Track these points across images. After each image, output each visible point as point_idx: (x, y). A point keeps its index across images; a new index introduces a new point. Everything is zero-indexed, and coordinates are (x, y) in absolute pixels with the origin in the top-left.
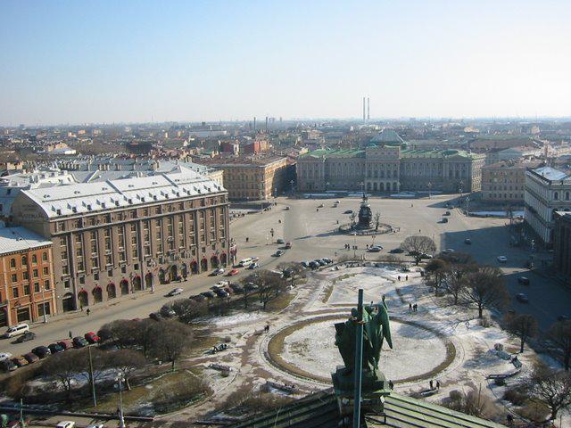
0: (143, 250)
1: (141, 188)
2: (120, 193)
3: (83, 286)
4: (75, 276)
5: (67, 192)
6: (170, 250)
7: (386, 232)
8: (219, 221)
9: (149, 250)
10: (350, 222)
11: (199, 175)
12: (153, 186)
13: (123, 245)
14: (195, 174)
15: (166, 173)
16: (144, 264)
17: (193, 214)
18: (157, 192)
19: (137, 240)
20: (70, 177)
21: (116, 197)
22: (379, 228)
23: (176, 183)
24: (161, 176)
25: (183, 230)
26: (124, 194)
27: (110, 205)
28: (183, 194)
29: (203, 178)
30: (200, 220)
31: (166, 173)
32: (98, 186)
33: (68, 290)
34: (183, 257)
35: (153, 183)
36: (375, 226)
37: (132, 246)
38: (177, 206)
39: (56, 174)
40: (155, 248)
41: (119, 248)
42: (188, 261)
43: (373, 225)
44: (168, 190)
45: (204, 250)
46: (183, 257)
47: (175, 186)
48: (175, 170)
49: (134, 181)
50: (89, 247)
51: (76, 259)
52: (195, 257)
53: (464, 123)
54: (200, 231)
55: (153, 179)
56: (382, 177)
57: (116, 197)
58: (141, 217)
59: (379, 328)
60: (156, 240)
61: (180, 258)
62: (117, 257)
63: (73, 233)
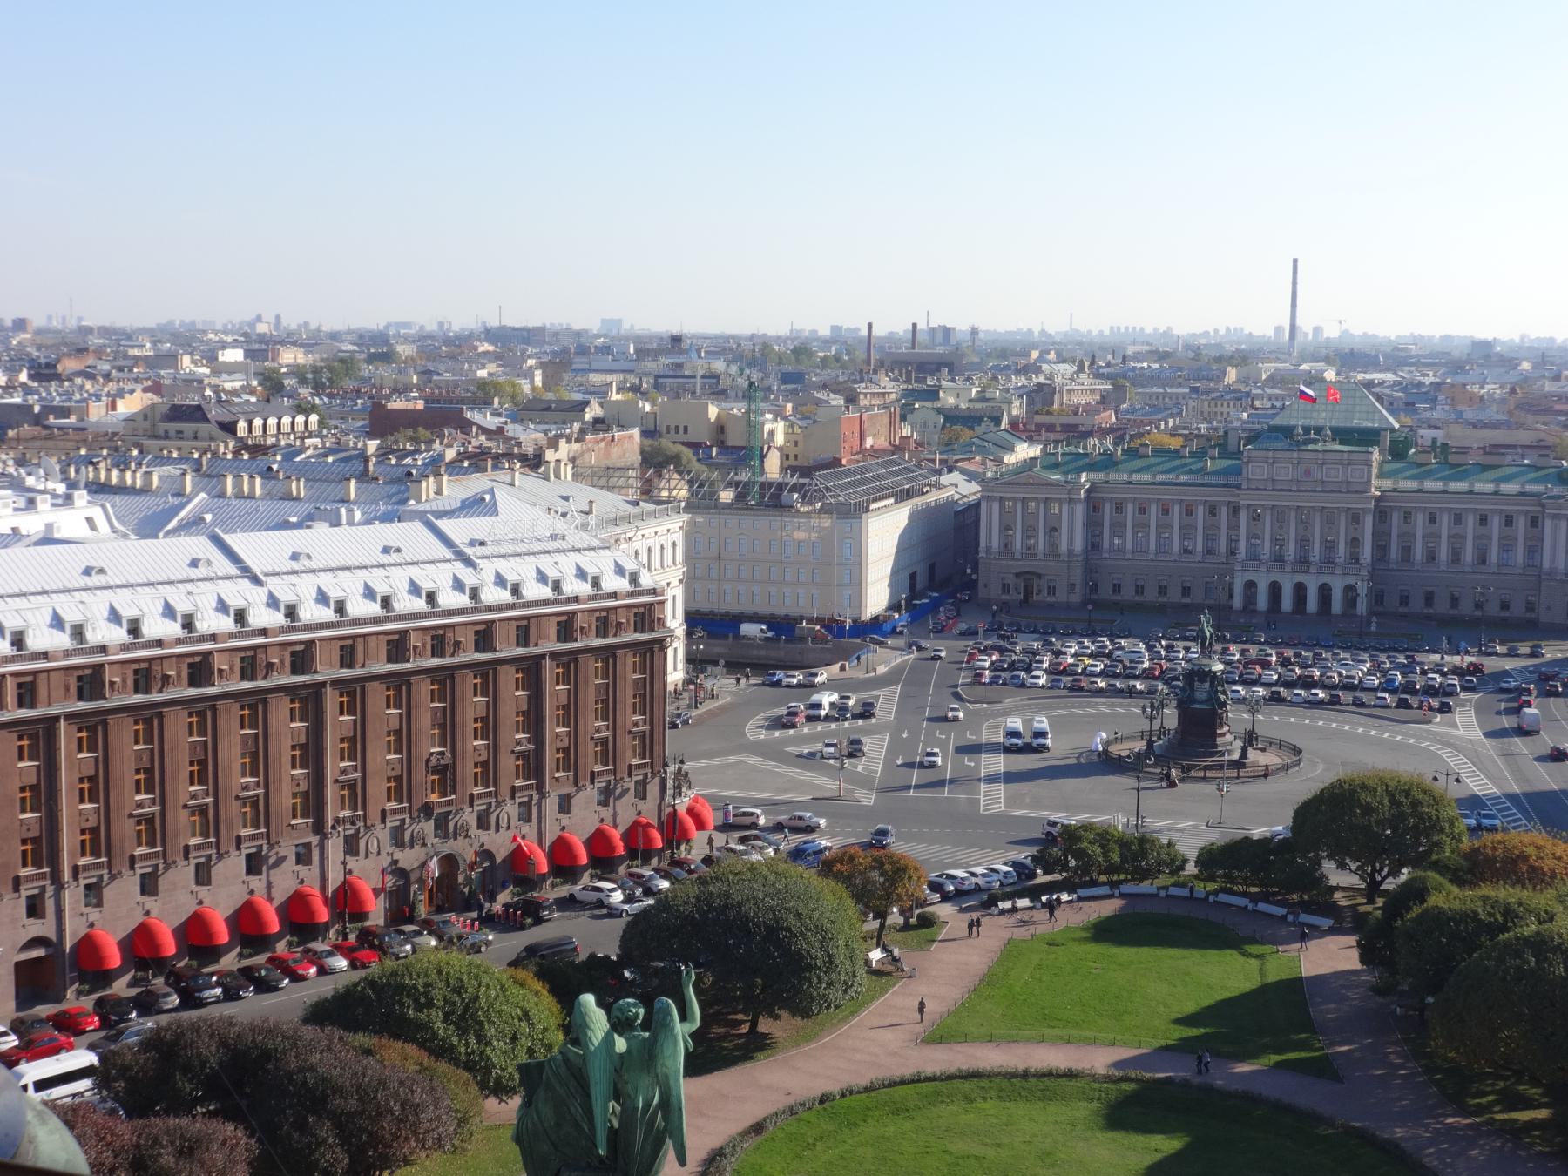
0: (331, 792)
1: (342, 568)
2: (256, 580)
3: (94, 914)
4: (67, 875)
5: (60, 566)
6: (434, 798)
7: (1286, 768)
8: (627, 696)
9: (355, 793)
10: (1145, 725)
11: (561, 526)
12: (386, 559)
13: (254, 773)
14: (547, 524)
15: (441, 514)
16: (335, 846)
17: (531, 670)
18: (394, 582)
19: (311, 753)
20: (97, 513)
21: (239, 593)
22: (1253, 756)
23: (469, 551)
24: (417, 527)
25: (488, 726)
26: (273, 584)
27: (211, 622)
28: (493, 595)
29: (577, 538)
30: (555, 691)
31: (441, 514)
32: (173, 552)
33: (36, 928)
34: (483, 823)
35: (386, 550)
36: (1239, 744)
37: (290, 777)
38: (467, 638)
39: (44, 503)
40: (377, 788)
41: (239, 781)
42: (500, 844)
43: (1230, 743)
44: (439, 578)
45: (565, 805)
46: (483, 823)
47: (469, 562)
48: (477, 505)
49: (322, 541)
50: (125, 770)
51: (73, 812)
52: (529, 830)
53: (1484, 355)
54: (555, 731)
55: (391, 532)
56: (1303, 560)
57: (239, 593)
58: (327, 670)
60: (383, 758)
61: (474, 830)
62: (181, 820)
63: (69, 717)
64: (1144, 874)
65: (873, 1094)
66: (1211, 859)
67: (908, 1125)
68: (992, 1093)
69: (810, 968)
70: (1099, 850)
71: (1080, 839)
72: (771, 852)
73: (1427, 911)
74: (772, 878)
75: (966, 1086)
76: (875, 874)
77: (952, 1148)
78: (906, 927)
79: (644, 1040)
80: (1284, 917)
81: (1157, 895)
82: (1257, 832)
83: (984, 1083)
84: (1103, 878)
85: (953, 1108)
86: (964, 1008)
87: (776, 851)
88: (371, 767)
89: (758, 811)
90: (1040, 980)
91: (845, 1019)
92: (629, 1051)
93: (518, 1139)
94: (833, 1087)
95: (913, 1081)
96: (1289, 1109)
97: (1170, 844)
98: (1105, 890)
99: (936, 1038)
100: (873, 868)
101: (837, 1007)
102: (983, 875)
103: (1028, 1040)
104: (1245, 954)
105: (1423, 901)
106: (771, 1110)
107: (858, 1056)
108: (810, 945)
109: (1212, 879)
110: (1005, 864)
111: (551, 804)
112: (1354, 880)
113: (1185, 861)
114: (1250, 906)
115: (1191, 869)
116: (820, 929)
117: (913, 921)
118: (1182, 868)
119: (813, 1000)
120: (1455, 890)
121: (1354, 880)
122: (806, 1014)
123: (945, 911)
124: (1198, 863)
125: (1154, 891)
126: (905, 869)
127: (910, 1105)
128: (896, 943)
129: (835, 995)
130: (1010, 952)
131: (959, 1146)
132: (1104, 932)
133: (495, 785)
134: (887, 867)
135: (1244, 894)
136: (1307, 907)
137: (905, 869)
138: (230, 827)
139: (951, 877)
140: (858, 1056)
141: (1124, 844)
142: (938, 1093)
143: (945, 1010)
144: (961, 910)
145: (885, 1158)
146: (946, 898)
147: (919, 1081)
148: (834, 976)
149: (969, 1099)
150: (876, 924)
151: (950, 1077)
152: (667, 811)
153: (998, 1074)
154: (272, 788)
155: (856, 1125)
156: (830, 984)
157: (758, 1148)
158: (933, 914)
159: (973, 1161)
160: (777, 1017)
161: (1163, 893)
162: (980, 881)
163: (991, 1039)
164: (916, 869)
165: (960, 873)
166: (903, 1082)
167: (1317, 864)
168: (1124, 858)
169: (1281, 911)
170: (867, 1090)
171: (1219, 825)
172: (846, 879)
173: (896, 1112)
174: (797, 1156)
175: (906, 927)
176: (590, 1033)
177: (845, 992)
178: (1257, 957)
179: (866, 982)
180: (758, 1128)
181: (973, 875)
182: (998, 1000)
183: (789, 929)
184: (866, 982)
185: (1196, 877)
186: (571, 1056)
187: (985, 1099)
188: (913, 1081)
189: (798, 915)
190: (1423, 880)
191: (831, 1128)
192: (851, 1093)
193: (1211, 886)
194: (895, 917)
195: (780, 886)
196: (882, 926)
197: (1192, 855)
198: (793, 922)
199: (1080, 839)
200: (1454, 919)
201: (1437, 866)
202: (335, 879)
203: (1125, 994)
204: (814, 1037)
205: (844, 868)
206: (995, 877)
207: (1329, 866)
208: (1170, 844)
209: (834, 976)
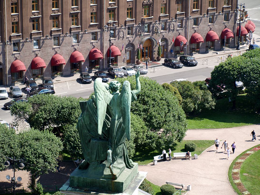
0: (106, 14)
4: (7, 39)
6: (145, 17)
45: (196, 22)
88: (121, 4)
111: (191, 23)
133: (169, 13)
138: (67, 24)
152: (237, 27)
154: (83, 10)
202: (106, 45)
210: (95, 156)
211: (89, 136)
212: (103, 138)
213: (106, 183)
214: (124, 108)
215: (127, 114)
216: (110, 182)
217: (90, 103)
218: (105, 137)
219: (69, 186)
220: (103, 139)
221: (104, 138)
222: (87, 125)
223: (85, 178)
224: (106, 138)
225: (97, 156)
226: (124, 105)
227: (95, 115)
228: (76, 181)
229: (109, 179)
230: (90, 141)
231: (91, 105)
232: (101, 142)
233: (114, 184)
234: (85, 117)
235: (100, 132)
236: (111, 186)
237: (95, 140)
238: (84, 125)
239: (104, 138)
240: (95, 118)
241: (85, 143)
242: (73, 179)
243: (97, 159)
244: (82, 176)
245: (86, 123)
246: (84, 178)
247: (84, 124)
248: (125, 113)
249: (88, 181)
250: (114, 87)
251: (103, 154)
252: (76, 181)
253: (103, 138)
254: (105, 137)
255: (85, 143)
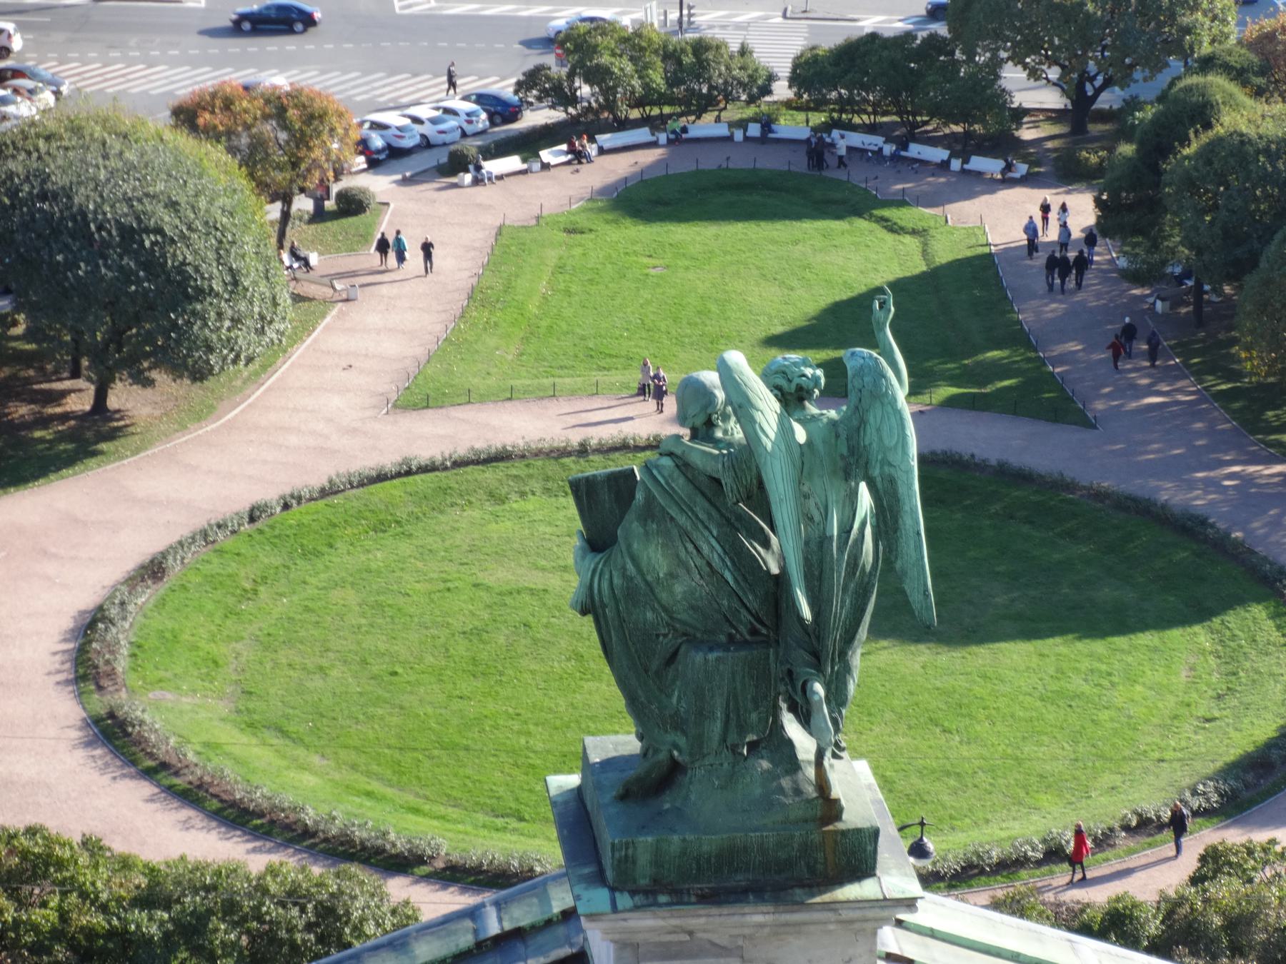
59: (853, 497)
64: (704, 104)
65: (336, 500)
66: (813, 73)
67: (405, 548)
68: (536, 485)
69: (201, 294)
70: (629, 68)
71: (594, 50)
72: (47, 97)
73: (1219, 140)
74: (115, 145)
75: (489, 475)
76: (268, 128)
77: (488, 580)
78: (320, 215)
79: (833, 423)
80: (945, 165)
81: (729, 139)
82: (870, 23)
83: (517, 469)
84: (635, 114)
85: (476, 514)
86: (453, 345)
87: (57, 94)
89: (9, 26)
90: (568, 293)
91: (255, 380)
92: (809, 443)
93: (588, 606)
94: (269, 494)
95: (399, 475)
96: (1022, 477)
97: (744, 51)
98: (643, 134)
99: (418, 396)
100: (266, 117)
101: (250, 360)
102: (434, 121)
103: (573, 393)
104: (894, 228)
105: (1208, 126)
106: (174, 538)
107: (293, 440)
108: (196, 254)
109: (817, 106)
110: (466, 98)
112: (1052, 99)
113: (771, 78)
114: (888, 149)
115: (782, 90)
116: (211, 226)
117: (330, 205)
118: (766, 90)
119: (210, 349)
120: (1260, 107)
121: (1052, 99)
122: (199, 374)
123: (379, 185)
124: (794, 80)
125: (723, 130)
126: (322, 117)
127: (401, 514)
128: (313, 244)
129: (243, 338)
130: (508, 246)
131: (499, 576)
132: (639, 201)
134: (292, 113)
135: (872, 129)
136: (964, 146)
137: (322, 117)
139: (377, 126)
140: (293, 440)
141: (670, 56)
142: (445, 491)
143: (420, 352)
144: (405, 182)
145: (379, 606)
146: (374, 164)
147: (409, 473)
148: (242, 306)
149: (496, 498)
150: (275, 211)
151: (459, 464)
153: (538, 453)
155: (317, 554)
156: (236, 321)
157: (161, 604)
158: (364, 191)
159: (527, 597)
160: (148, 383)
161: (738, 135)
162: (427, 129)
163: (511, 396)
164: (341, 115)
165: (393, 119)
166: (381, 477)
167: (995, 66)
168: (672, 82)
169: (939, 154)
170: (324, 493)
171: (805, 15)
172: (224, 136)
173: (380, 527)
174: (230, 613)
175: (320, 215)
176: (758, 416)
177: (261, 332)
178: (914, 232)
179: (291, 314)
180: (153, 570)
181: (416, 120)
182: (501, 324)
183: (159, 231)
184: (291, 314)
185: (788, 105)
186: (696, 460)
187: (523, 494)
188: (399, 475)
189: (173, 205)
190: (1202, 90)
191: (277, 561)
192: (299, 499)
193: (819, 118)
194: (303, 204)
195: (131, 156)
196: (286, 216)
197: (783, 68)
198: (167, 219)
199: (594, 50)
200: (1266, 151)
201: (1207, 64)
203: (714, 308)
204: (201, 414)
205: (218, 120)
206: (452, 123)
207: (1012, 76)
208: (744, 51)
209: (242, 306)
210: (715, 728)
211: (665, 636)
212: (748, 637)
213: (796, 846)
214: (892, 481)
215: (907, 508)
216: (816, 837)
217: (663, 477)
218: (758, 626)
219: (613, 890)
220: (746, 642)
221: (754, 632)
222: (654, 585)
223: (690, 837)
224: (764, 631)
225: (733, 723)
226: (890, 465)
227: (706, 533)
228: (644, 859)
229: (806, 821)
230: (672, 658)
231: (672, 488)
232: (743, 653)
233: (836, 841)
234: (635, 546)
235: (806, 613)
236: (820, 855)
237: (711, 650)
238: (642, 585)
239: (754, 632)
240: (709, 543)
241: (646, 671)
242: (630, 852)
243: (732, 738)
244: (675, 832)
245: (649, 578)
246: (684, 840)
247: (638, 580)
248: (898, 500)
249: (705, 848)
250: (800, 388)
251: (756, 708)
252: (644, 859)
253: (748, 637)
254: (758, 626)
255: (646, 671)
